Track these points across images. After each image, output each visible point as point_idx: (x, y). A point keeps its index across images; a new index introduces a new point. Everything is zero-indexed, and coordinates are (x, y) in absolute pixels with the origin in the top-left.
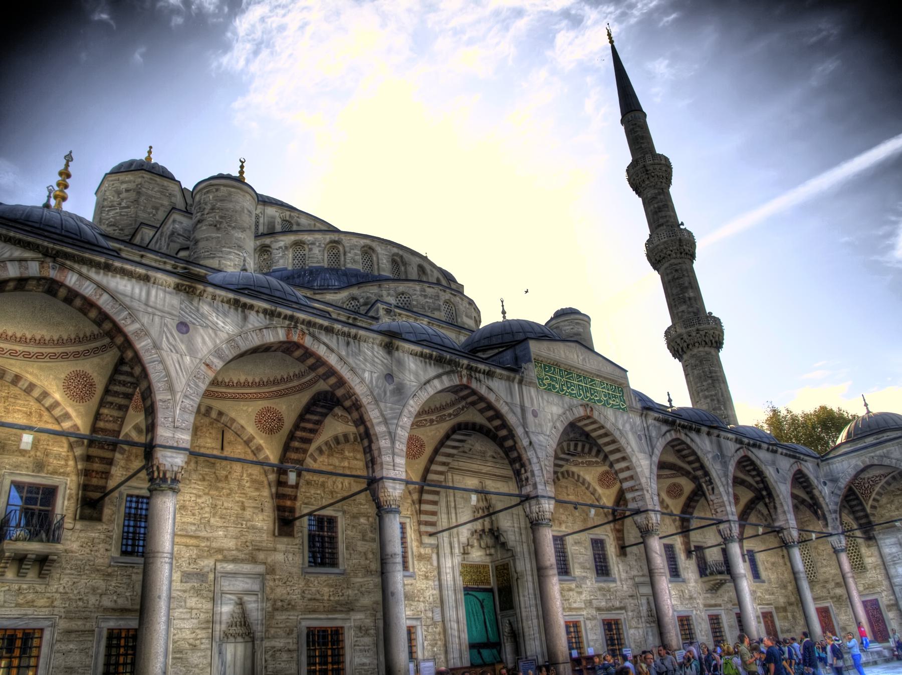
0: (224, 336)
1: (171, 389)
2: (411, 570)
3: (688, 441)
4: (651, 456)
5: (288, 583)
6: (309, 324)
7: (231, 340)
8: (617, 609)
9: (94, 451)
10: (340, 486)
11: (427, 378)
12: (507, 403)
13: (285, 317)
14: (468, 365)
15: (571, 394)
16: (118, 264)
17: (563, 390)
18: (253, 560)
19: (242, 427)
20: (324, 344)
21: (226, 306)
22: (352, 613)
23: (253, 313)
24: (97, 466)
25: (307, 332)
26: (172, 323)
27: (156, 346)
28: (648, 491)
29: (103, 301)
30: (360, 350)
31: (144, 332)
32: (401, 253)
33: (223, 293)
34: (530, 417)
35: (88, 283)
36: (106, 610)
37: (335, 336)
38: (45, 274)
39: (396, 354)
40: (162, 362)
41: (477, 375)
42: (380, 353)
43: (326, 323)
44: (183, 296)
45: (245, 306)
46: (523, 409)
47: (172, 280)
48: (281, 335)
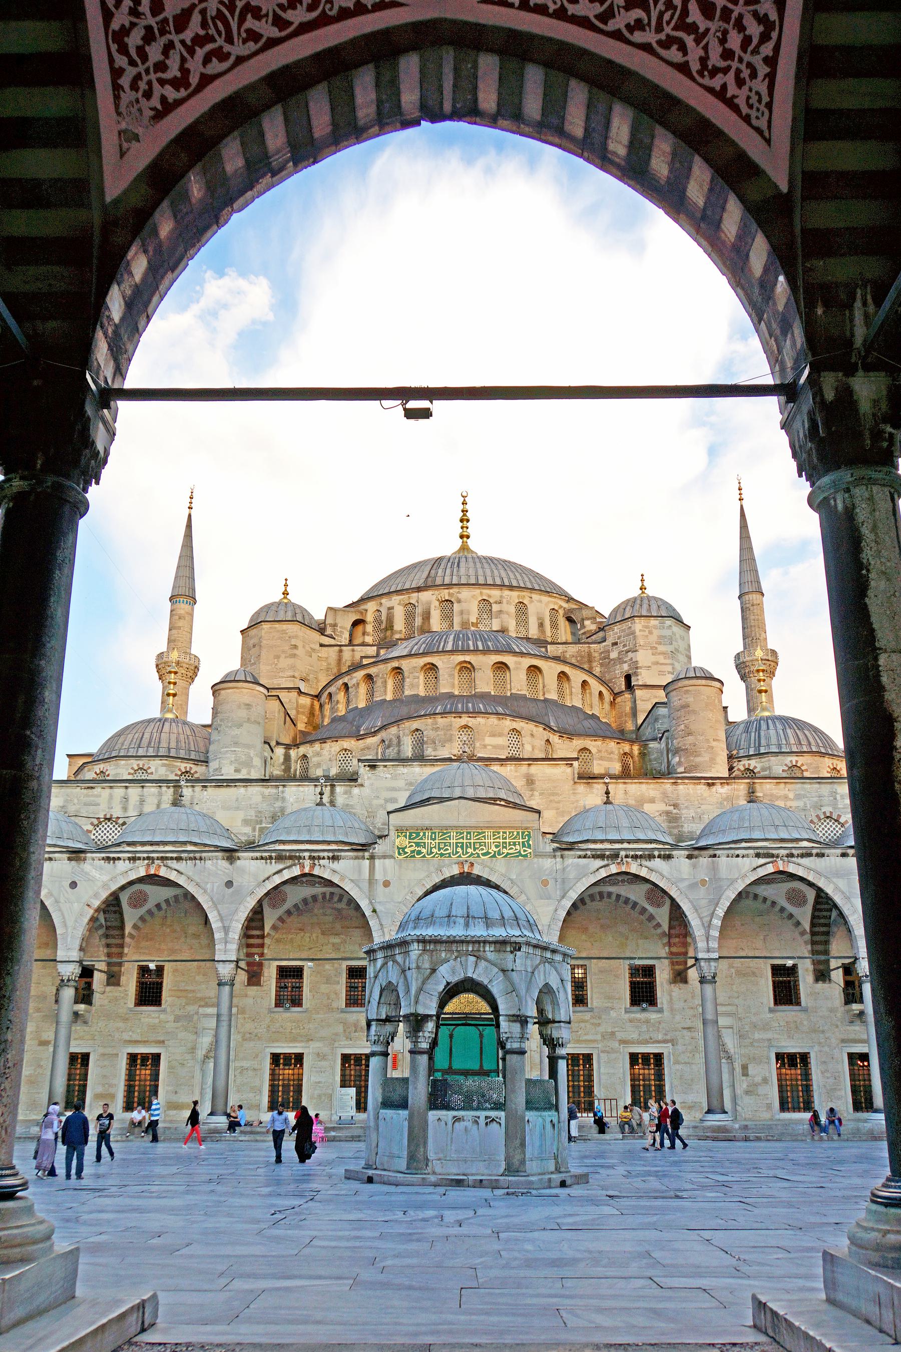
0: (99, 884)
1: (65, 926)
3: (643, 873)
4: (559, 901)
6: (162, 859)
7: (105, 886)
8: (659, 1042)
9: (111, 941)
12: (352, 881)
15: (442, 855)
24: (114, 950)
32: (467, 658)
34: (380, 888)
41: (322, 862)
42: (225, 864)
43: (175, 855)
45: (114, 859)
46: (372, 881)
47: (66, 856)
48: (142, 873)
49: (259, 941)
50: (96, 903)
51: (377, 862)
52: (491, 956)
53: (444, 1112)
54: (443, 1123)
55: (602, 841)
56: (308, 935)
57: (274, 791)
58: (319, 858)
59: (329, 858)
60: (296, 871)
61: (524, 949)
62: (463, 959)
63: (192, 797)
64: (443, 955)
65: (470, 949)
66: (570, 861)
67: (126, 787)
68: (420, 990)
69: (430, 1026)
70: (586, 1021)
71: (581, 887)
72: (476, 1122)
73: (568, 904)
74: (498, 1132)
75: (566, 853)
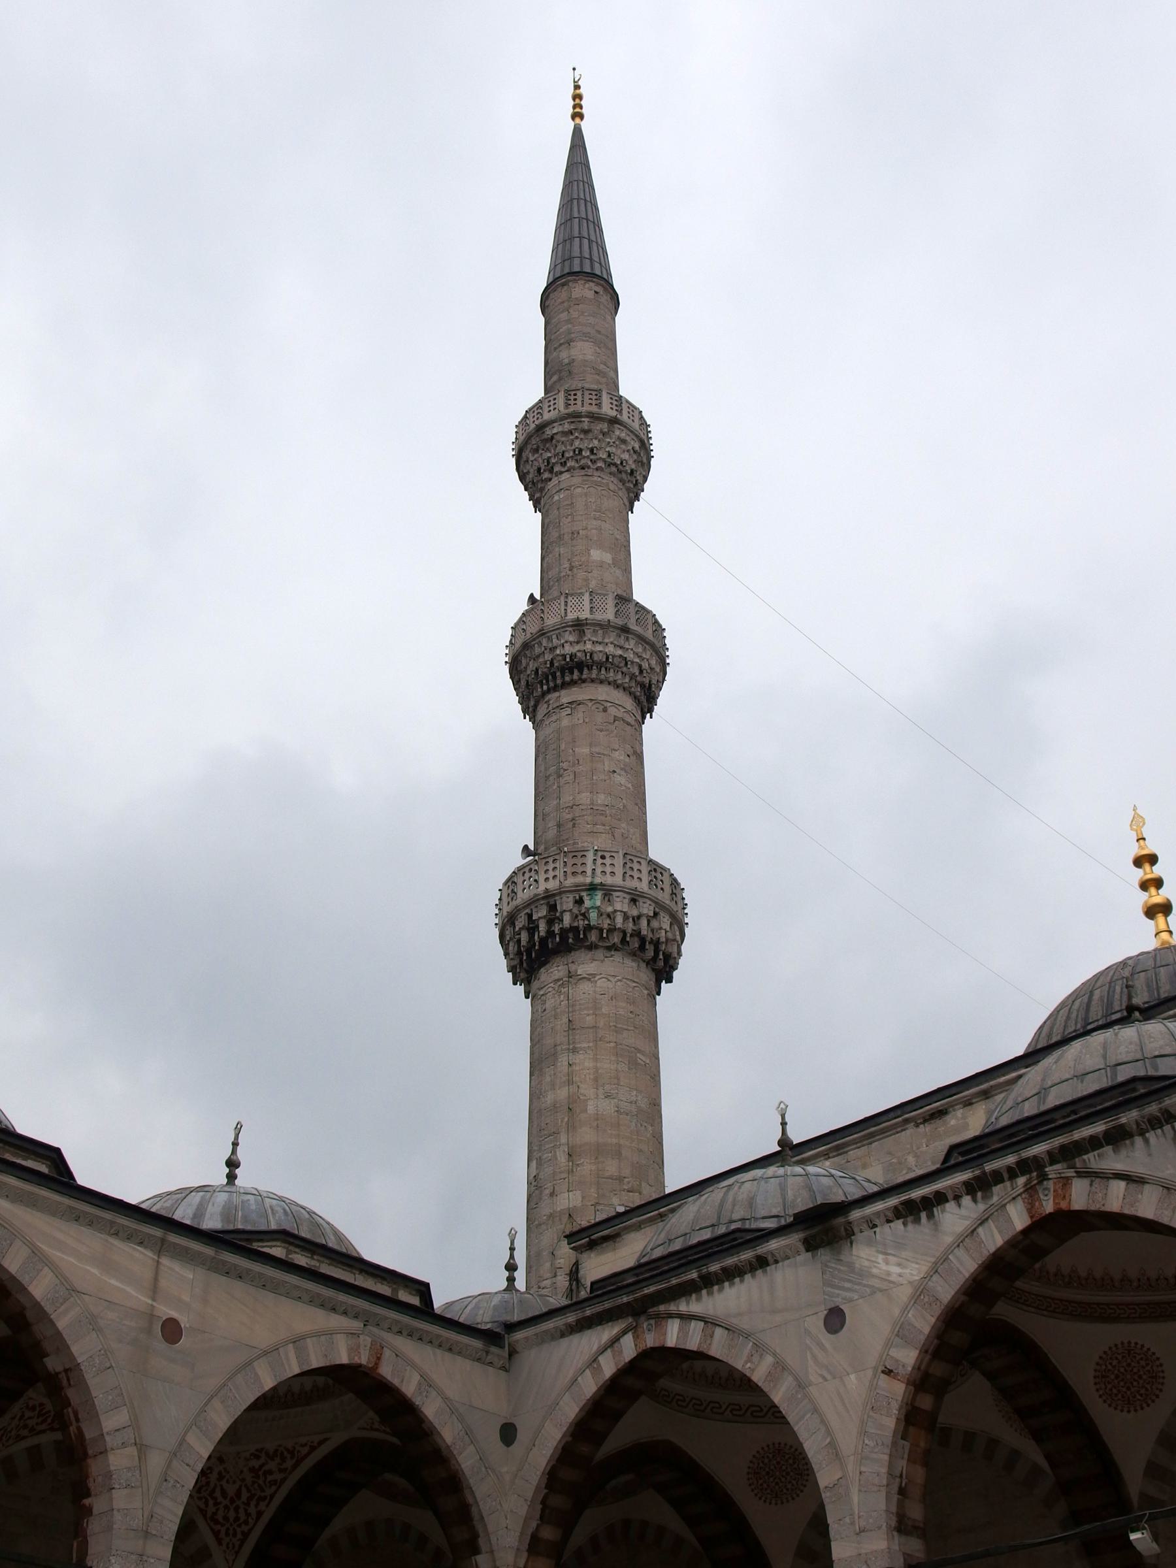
0: (904, 1294)
1: (836, 1454)
6: (1068, 1153)
7: (920, 1292)
20: (1119, 1176)
21: (898, 1225)
23: (951, 1206)
25: (1070, 1173)
26: (816, 1323)
27: (801, 1385)
29: (718, 1346)
31: (780, 1366)
33: (879, 1206)
35: (693, 1323)
37: (1138, 1140)
38: (642, 1347)
40: (816, 1410)
44: (824, 1254)
47: (794, 1239)
48: (1018, 1218)
50: (907, 1357)
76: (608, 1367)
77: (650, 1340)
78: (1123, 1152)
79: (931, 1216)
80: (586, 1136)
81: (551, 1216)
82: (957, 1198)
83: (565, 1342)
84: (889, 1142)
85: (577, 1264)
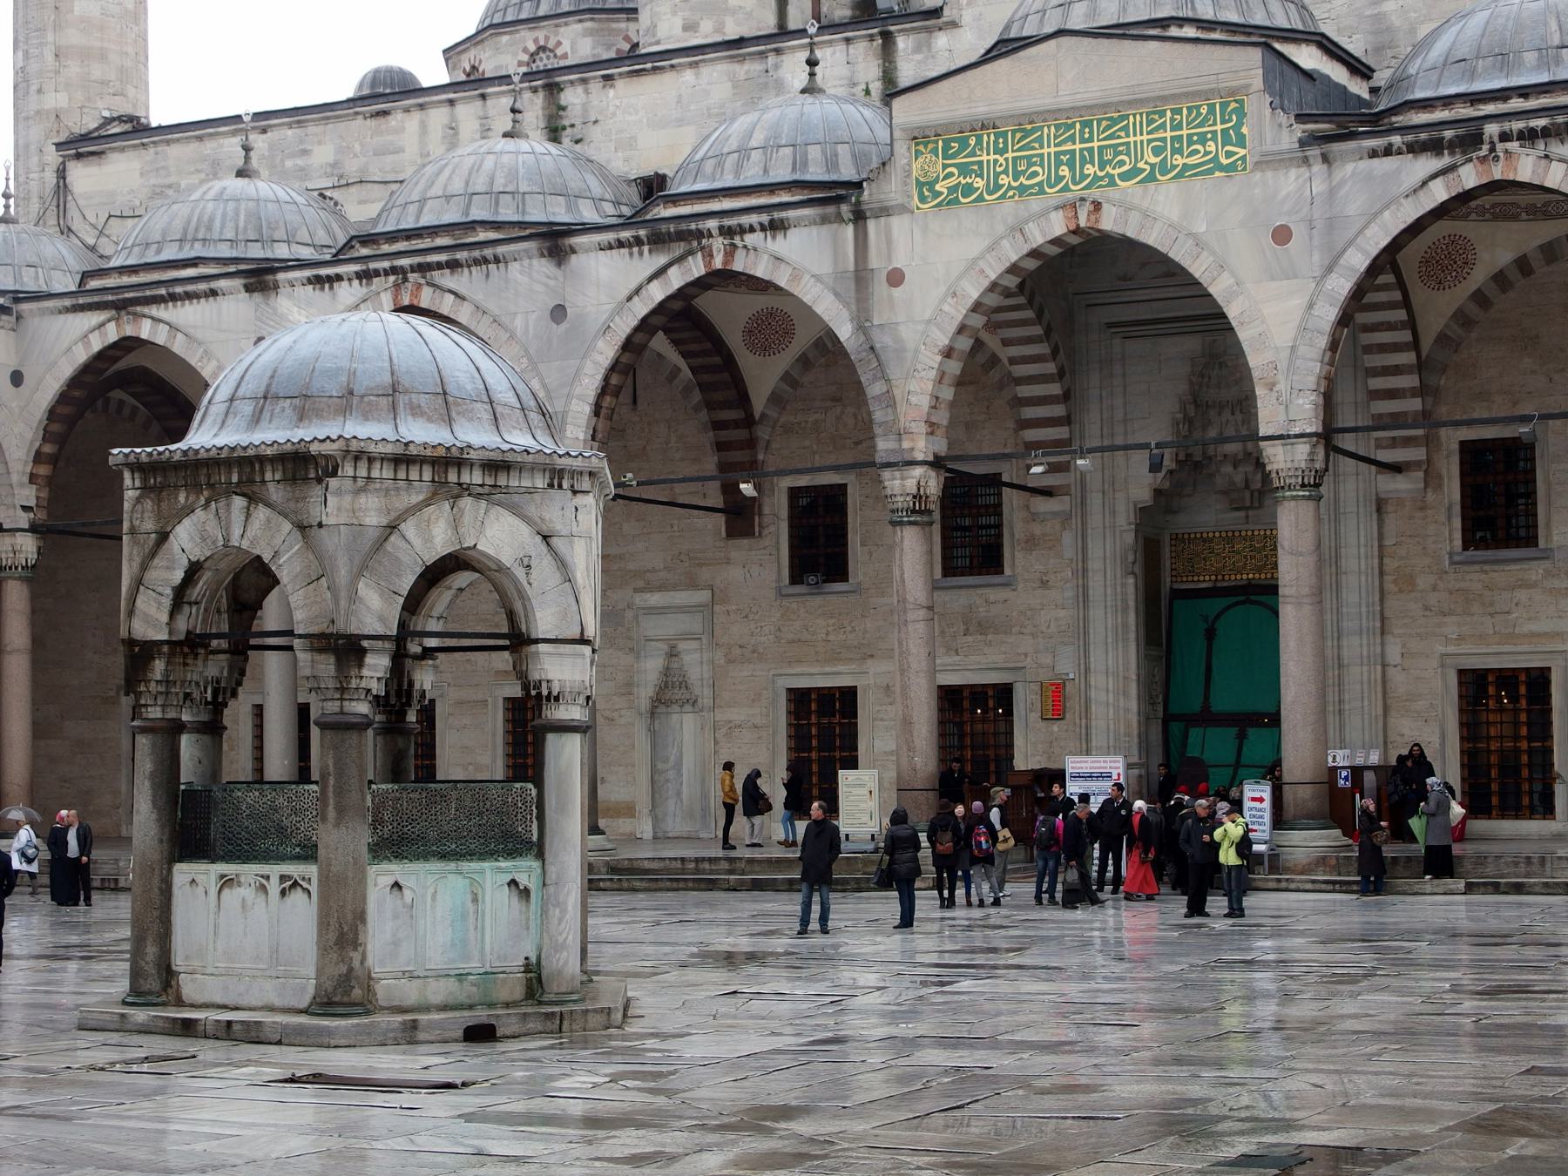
2: (1007, 571)
5: (751, 616)
6: (422, 268)
10: (851, 422)
11: (633, 286)
13: (387, 273)
14: (721, 228)
15: (1022, 190)
16: (179, 289)
17: (998, 187)
18: (693, 585)
19: (659, 355)
22: (870, 662)
23: (345, 284)
25: (422, 281)
28: (1271, 386)
29: (178, 346)
30: (507, 281)
34: (880, 287)
36: (498, 672)
39: (574, 257)
41: (750, 239)
43: (443, 257)
44: (257, 296)
46: (861, 277)
47: (238, 283)
49: (739, 434)
51: (871, 225)
52: (275, 492)
53: (202, 867)
54: (200, 890)
55: (1448, 101)
56: (850, 410)
57: (754, 67)
58: (742, 230)
59: (763, 228)
60: (697, 267)
61: (349, 470)
62: (222, 504)
63: (585, 107)
64: (182, 498)
65: (235, 479)
66: (1350, 168)
67: (451, 102)
68: (138, 583)
69: (159, 666)
70: (1534, 585)
71: (1378, 238)
72: (263, 888)
73: (1341, 285)
74: (302, 912)
75: (1336, 147)
76: (97, 344)
77: (129, 331)
78: (456, 276)
79: (331, 288)
80: (73, 37)
81: (38, 112)
82: (350, 280)
83: (62, 317)
84: (341, 126)
85: (61, 173)
